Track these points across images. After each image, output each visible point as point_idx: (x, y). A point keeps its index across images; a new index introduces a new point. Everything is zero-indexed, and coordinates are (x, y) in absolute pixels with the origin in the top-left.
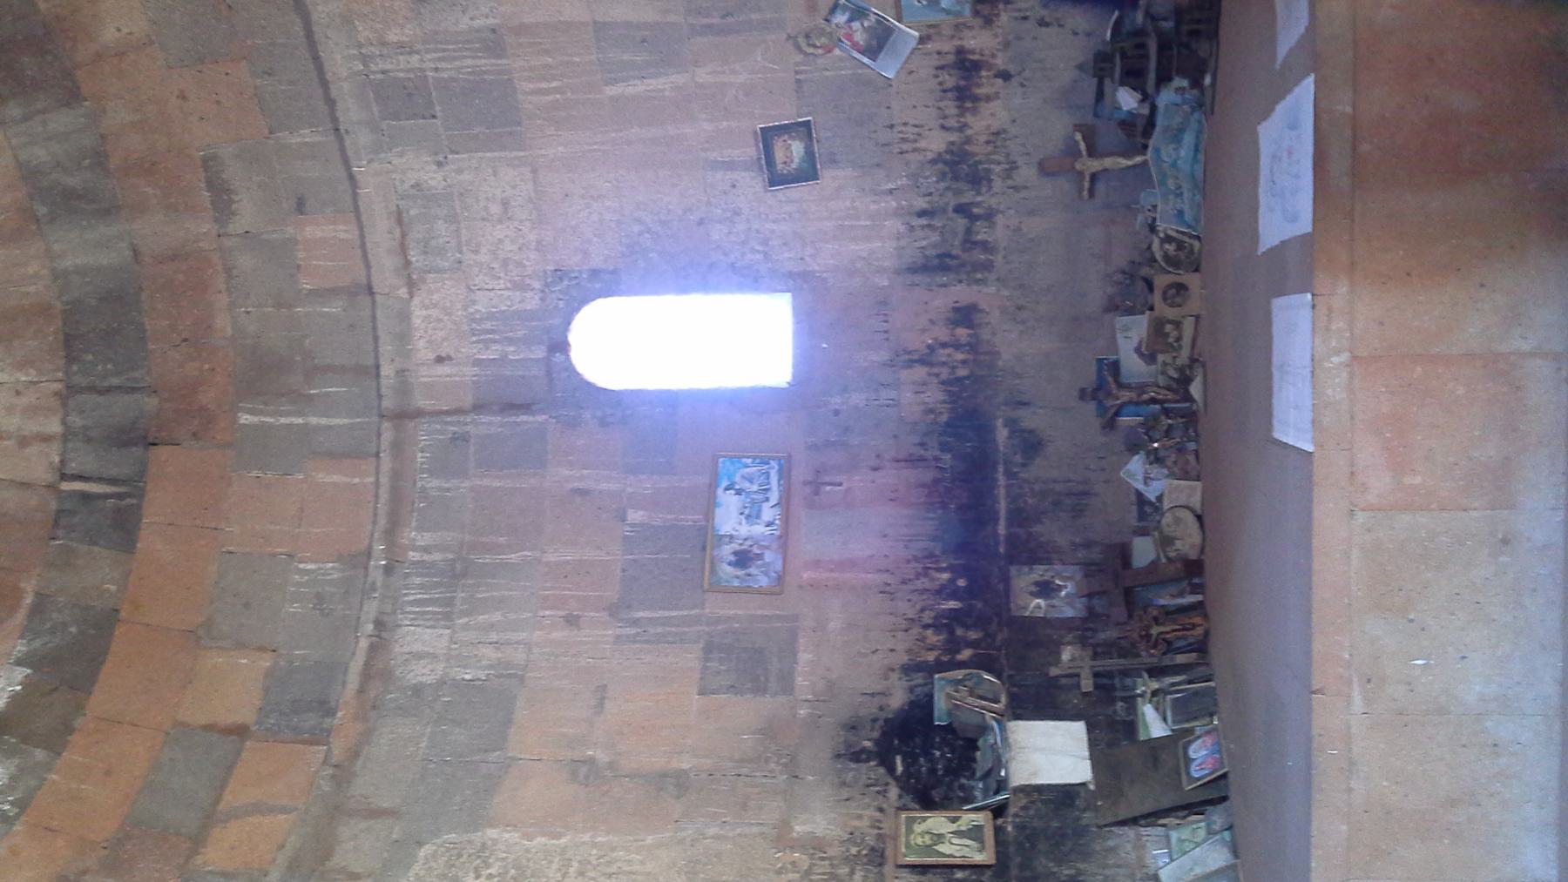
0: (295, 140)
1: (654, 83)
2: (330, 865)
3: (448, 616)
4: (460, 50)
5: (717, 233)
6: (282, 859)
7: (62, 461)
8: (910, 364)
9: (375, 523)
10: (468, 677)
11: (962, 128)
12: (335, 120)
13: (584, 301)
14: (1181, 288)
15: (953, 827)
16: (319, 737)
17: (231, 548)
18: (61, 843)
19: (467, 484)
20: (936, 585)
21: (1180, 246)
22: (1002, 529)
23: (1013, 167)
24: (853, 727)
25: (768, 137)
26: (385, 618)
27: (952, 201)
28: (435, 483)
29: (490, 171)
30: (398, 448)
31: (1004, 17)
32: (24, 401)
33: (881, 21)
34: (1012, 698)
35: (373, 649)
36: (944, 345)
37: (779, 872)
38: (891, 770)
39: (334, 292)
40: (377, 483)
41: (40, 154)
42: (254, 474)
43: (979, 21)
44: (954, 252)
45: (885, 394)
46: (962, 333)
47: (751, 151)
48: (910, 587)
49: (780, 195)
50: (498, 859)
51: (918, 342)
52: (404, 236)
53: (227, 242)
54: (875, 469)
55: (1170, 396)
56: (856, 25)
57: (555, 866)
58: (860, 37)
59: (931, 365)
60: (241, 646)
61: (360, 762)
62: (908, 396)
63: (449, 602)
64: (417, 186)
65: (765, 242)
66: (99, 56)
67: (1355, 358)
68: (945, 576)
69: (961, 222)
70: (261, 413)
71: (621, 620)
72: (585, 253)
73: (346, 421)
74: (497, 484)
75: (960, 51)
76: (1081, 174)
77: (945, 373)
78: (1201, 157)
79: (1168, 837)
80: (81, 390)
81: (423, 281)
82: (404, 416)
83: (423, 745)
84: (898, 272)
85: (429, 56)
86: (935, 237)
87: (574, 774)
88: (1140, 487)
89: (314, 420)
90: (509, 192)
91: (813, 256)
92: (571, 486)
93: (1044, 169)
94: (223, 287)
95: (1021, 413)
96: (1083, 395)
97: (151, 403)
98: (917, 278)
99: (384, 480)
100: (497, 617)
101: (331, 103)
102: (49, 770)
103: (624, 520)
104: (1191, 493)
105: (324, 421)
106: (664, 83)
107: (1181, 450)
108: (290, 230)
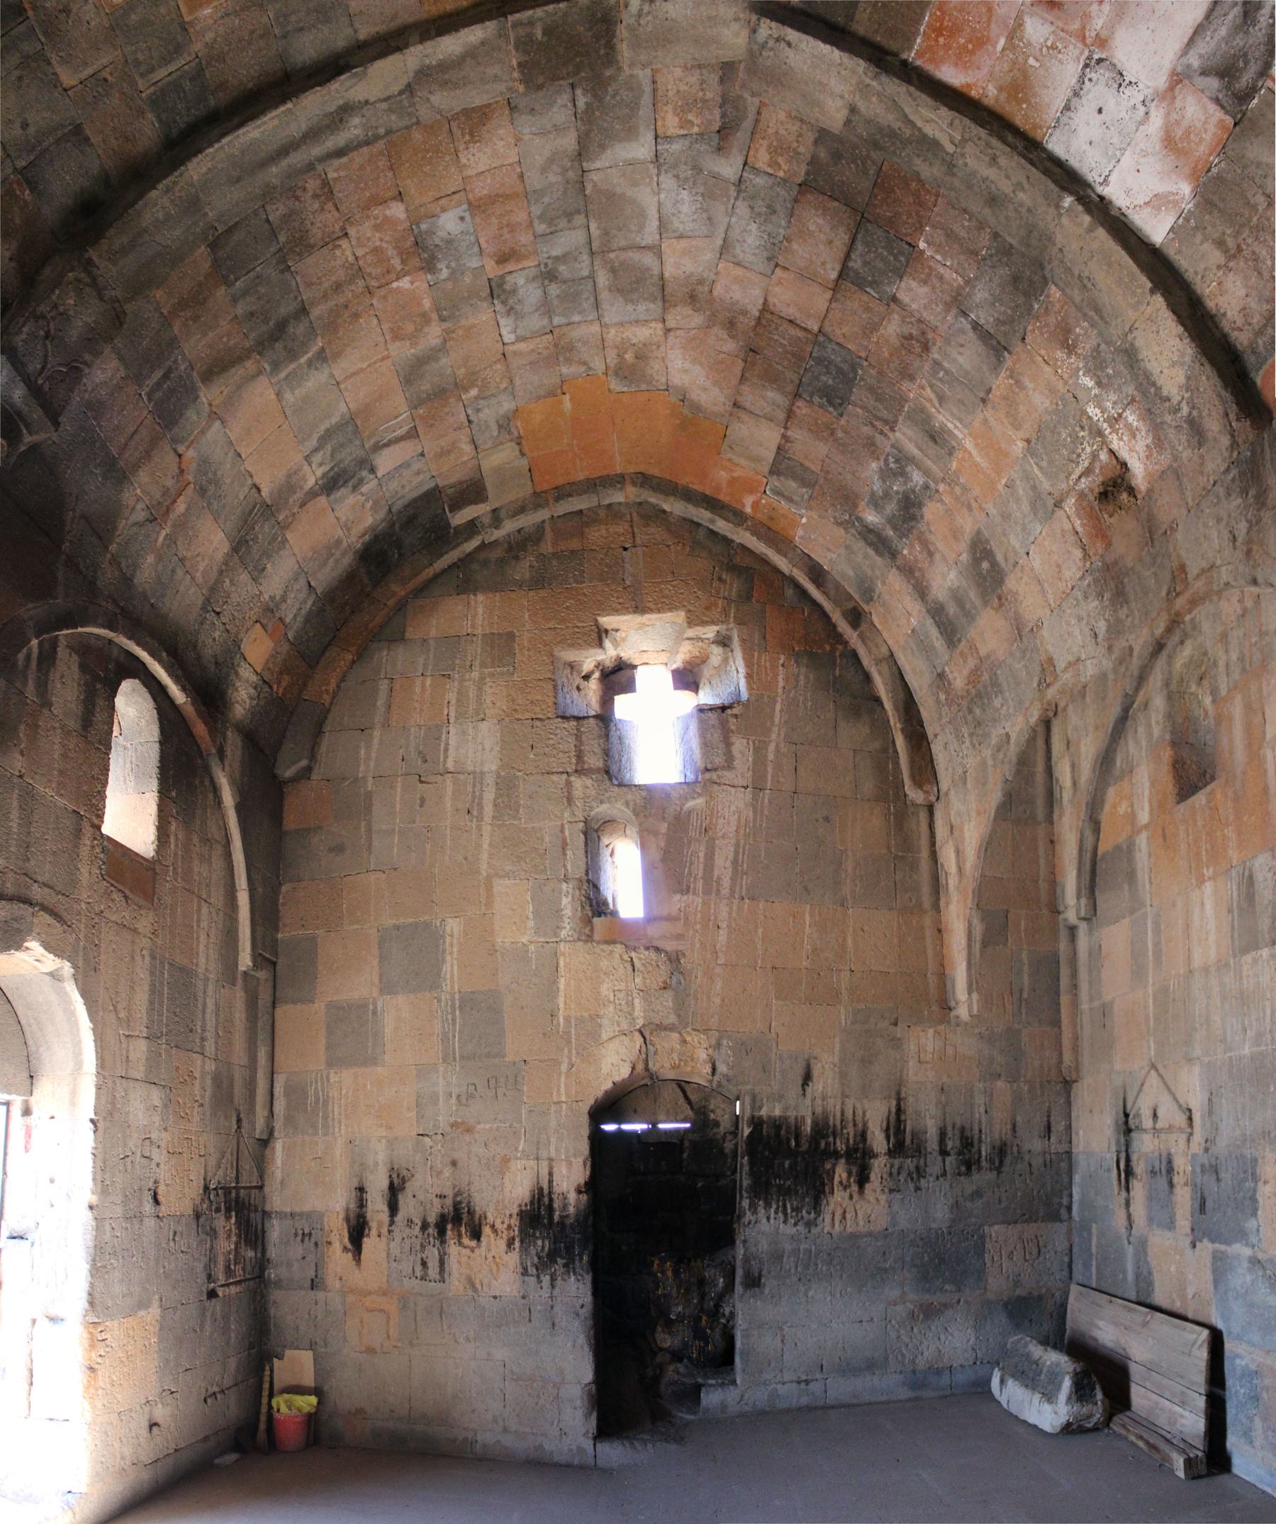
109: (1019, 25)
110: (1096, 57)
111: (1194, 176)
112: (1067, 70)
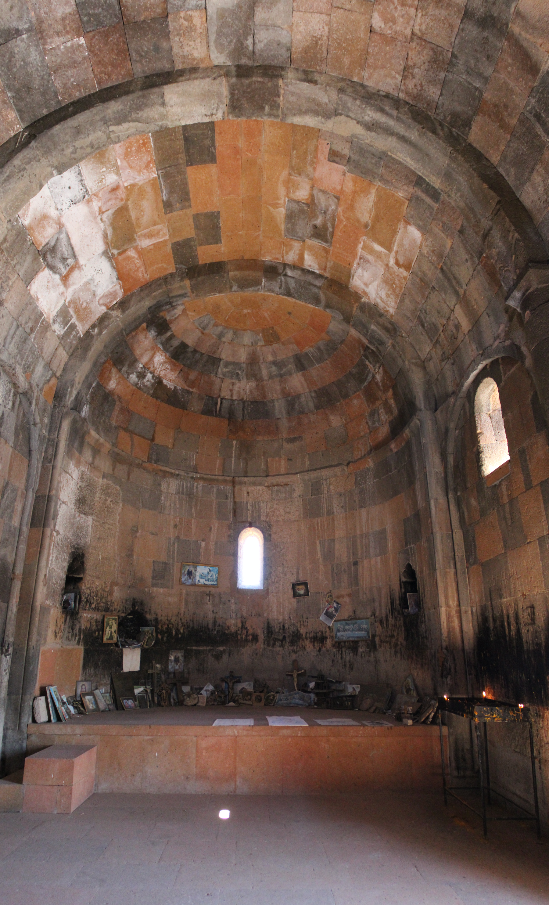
0: (306, 460)
1: (319, 553)
3: (179, 493)
5: (280, 569)
6: (120, 452)
7: (225, 399)
8: (242, 622)
9: (205, 474)
11: (306, 638)
12: (311, 470)
13: (263, 532)
14: (260, 700)
15: (113, 632)
16: (149, 460)
18: (129, 397)
19: (214, 499)
20: (179, 628)
21: (272, 700)
22: (194, 648)
23: (295, 652)
24: (142, 604)
25: (305, 584)
27: (287, 635)
28: (215, 490)
30: (225, 481)
31: (335, 650)
32: (242, 391)
33: (334, 616)
34: (147, 649)
35: (172, 473)
36: (247, 632)
37: (105, 583)
38: (129, 614)
39: (267, 467)
40: (216, 475)
41: (303, 399)
43: (334, 643)
44: (273, 636)
45: (234, 615)
46: (250, 637)
47: (302, 579)
48: (179, 621)
49: (290, 587)
51: (248, 625)
52: (281, 485)
53: (280, 441)
54: (213, 612)
55: (230, 697)
56: (333, 609)
57: (111, 522)
58: (330, 610)
59: (242, 628)
60: (175, 440)
61: (142, 470)
62: (233, 622)
63: (183, 494)
64: (294, 490)
65: (277, 582)
66: (327, 414)
67: (236, 736)
68: (182, 631)
69: (281, 638)
72: (276, 533)
74: (214, 507)
75: (326, 638)
76: (293, 672)
77: (239, 632)
78: (296, 706)
79: (107, 693)
80: (244, 404)
81: (269, 490)
82: (233, 483)
84: (268, 619)
86: (277, 630)
87: (134, 526)
88: (205, 689)
89: (233, 460)
90: (292, 514)
91: (273, 595)
92: (212, 526)
93: (295, 661)
94: (269, 439)
95: (227, 654)
96: (231, 672)
98: (266, 625)
99: (216, 477)
100: (178, 506)
101: (315, 470)
102: (147, 394)
104: (202, 702)
105: (233, 462)
106: (319, 556)
107: (215, 700)
109: (118, 174)
110: (87, 196)
111: (31, 228)
112: (91, 183)
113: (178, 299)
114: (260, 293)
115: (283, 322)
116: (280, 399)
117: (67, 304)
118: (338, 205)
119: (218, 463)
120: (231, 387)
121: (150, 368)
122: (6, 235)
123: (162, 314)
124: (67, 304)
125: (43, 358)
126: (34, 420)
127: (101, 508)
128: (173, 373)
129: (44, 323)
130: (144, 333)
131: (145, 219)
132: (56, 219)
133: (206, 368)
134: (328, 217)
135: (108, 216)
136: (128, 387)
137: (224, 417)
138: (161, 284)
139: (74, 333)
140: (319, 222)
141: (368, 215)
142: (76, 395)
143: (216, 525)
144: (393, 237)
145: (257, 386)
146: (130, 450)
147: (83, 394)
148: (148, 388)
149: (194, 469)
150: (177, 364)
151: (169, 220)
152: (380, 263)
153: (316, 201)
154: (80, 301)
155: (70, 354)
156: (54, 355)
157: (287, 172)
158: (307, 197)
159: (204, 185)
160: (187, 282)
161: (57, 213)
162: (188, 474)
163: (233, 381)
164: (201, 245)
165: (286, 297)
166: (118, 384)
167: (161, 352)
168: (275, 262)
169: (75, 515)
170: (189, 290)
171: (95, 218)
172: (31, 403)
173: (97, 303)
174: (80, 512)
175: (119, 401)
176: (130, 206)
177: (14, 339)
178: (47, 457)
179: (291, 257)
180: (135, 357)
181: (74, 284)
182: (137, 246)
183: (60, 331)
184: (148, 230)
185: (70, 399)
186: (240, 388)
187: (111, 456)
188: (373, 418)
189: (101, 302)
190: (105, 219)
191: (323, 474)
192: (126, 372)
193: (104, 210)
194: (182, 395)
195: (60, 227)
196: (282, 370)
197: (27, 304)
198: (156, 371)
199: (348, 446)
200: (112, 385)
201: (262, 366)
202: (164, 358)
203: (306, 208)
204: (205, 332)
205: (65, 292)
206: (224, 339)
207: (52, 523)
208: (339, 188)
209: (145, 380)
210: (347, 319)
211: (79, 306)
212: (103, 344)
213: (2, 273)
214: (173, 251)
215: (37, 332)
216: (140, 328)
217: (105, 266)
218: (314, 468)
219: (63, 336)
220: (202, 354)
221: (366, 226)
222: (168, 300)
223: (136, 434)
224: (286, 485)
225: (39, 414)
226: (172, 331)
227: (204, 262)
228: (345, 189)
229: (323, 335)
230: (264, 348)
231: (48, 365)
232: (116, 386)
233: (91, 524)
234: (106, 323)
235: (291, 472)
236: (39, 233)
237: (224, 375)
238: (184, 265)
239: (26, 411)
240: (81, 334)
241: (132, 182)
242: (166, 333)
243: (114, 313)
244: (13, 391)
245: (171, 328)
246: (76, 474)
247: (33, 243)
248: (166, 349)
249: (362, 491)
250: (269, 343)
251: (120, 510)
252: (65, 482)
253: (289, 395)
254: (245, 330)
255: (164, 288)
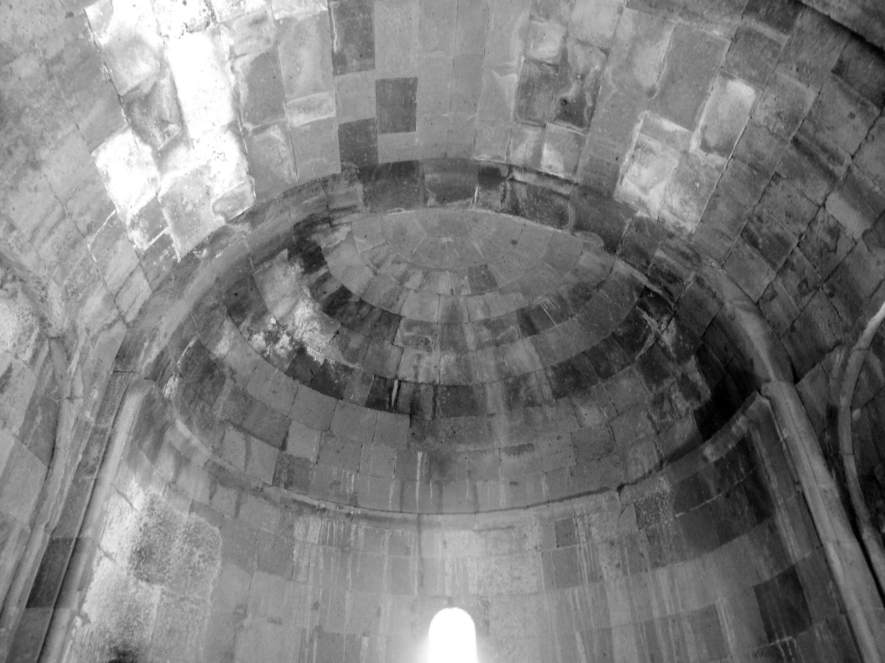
2: (219, 485)
3: (324, 543)
4: (590, 561)
9: (370, 509)
10: (294, 552)
12: (553, 501)
16: (276, 481)
17: (363, 446)
18: (249, 372)
19: (386, 554)
26: (326, 513)
28: (387, 538)
29: (535, 572)
30: (405, 521)
32: (432, 369)
35: (313, 507)
39: (476, 496)
40: (389, 511)
41: (533, 381)
42: (396, 457)
50: (206, 566)
52: (502, 529)
57: (198, 597)
60: (321, 449)
63: (331, 544)
64: (525, 536)
70: (422, 461)
71: (313, 632)
73: (417, 499)
74: (385, 568)
83: (266, 530)
85: (586, 546)
87: (240, 607)
89: (418, 484)
92: (382, 606)
97: (428, 417)
99: (390, 515)
100: (321, 567)
101: (561, 500)
102: (280, 369)
103: (364, 635)
105: (417, 488)
108: (503, 478)
110: (212, 24)
111: (108, 52)
113: (342, 214)
114: (470, 210)
115: (503, 257)
116: (494, 382)
117: (160, 200)
118: (605, 63)
119: (393, 490)
120: (415, 363)
121: (287, 326)
122: (63, 51)
123: (314, 237)
124: (160, 200)
125: (105, 284)
126: (72, 389)
127: (181, 568)
128: (323, 336)
129: (115, 222)
130: (285, 266)
131: (302, 80)
132: (157, 50)
133: (377, 330)
134: (588, 83)
135: (244, 64)
136: (249, 355)
137: (402, 413)
138: (317, 189)
139: (166, 252)
140: (570, 94)
141: (655, 75)
142: (158, 356)
143: (389, 604)
144: (699, 104)
145: (458, 360)
146: (243, 464)
147: (171, 357)
148: (282, 359)
149: (351, 500)
150: (332, 322)
151: (339, 87)
152: (673, 150)
153: (569, 60)
154: (182, 199)
155: (155, 287)
156: (126, 283)
157: (528, 15)
158: (555, 55)
159: (398, 33)
160: (359, 187)
161: (160, 40)
162: (341, 508)
163: (419, 352)
164: (384, 132)
165: (511, 216)
166: (232, 348)
167: (307, 301)
168: (495, 163)
169: (127, 582)
170: (361, 201)
171: (223, 63)
172: (69, 358)
173: (211, 208)
174: (139, 576)
175: (232, 378)
176: (280, 55)
177: (52, 238)
178: (87, 463)
179: (521, 154)
180: (265, 306)
181: (175, 168)
182: (286, 122)
183: (141, 244)
184: (305, 98)
185: (146, 361)
186: (429, 363)
187: (210, 472)
188: (661, 409)
189: (218, 208)
190: (237, 68)
191: (575, 506)
192: (248, 330)
193: (238, 52)
194: (337, 374)
195: (161, 65)
196: (499, 334)
197: (86, 182)
198: (297, 332)
199: (616, 457)
200: (222, 348)
201: (468, 329)
202: (312, 312)
203: (552, 72)
204: (379, 271)
205: (159, 178)
206: (408, 285)
207: (75, 597)
208: (609, 34)
209: (277, 346)
210: (611, 246)
211: (180, 207)
212: (215, 276)
213: (46, 114)
214: (340, 137)
215: (100, 235)
216: (278, 258)
217: (231, 148)
218: (558, 496)
219: (146, 254)
220: (372, 308)
221: (651, 93)
222: (326, 214)
223: (255, 436)
224: (511, 527)
225: (83, 381)
226: (327, 268)
227: (386, 161)
228: (620, 35)
229: (568, 275)
230: (470, 299)
231: (113, 299)
232: (229, 351)
233: (158, 601)
234: (223, 242)
235: (517, 505)
236: (124, 67)
237: (405, 343)
238: (355, 163)
239: (59, 372)
240: (178, 257)
241: (287, 14)
242: (318, 270)
243: (238, 228)
244: (37, 330)
245: (326, 263)
246: (139, 500)
247: (111, 81)
248: (315, 297)
249: (652, 537)
250: (478, 291)
251: (215, 575)
252: (117, 513)
253: (509, 375)
254: (441, 270)
255: (322, 194)
